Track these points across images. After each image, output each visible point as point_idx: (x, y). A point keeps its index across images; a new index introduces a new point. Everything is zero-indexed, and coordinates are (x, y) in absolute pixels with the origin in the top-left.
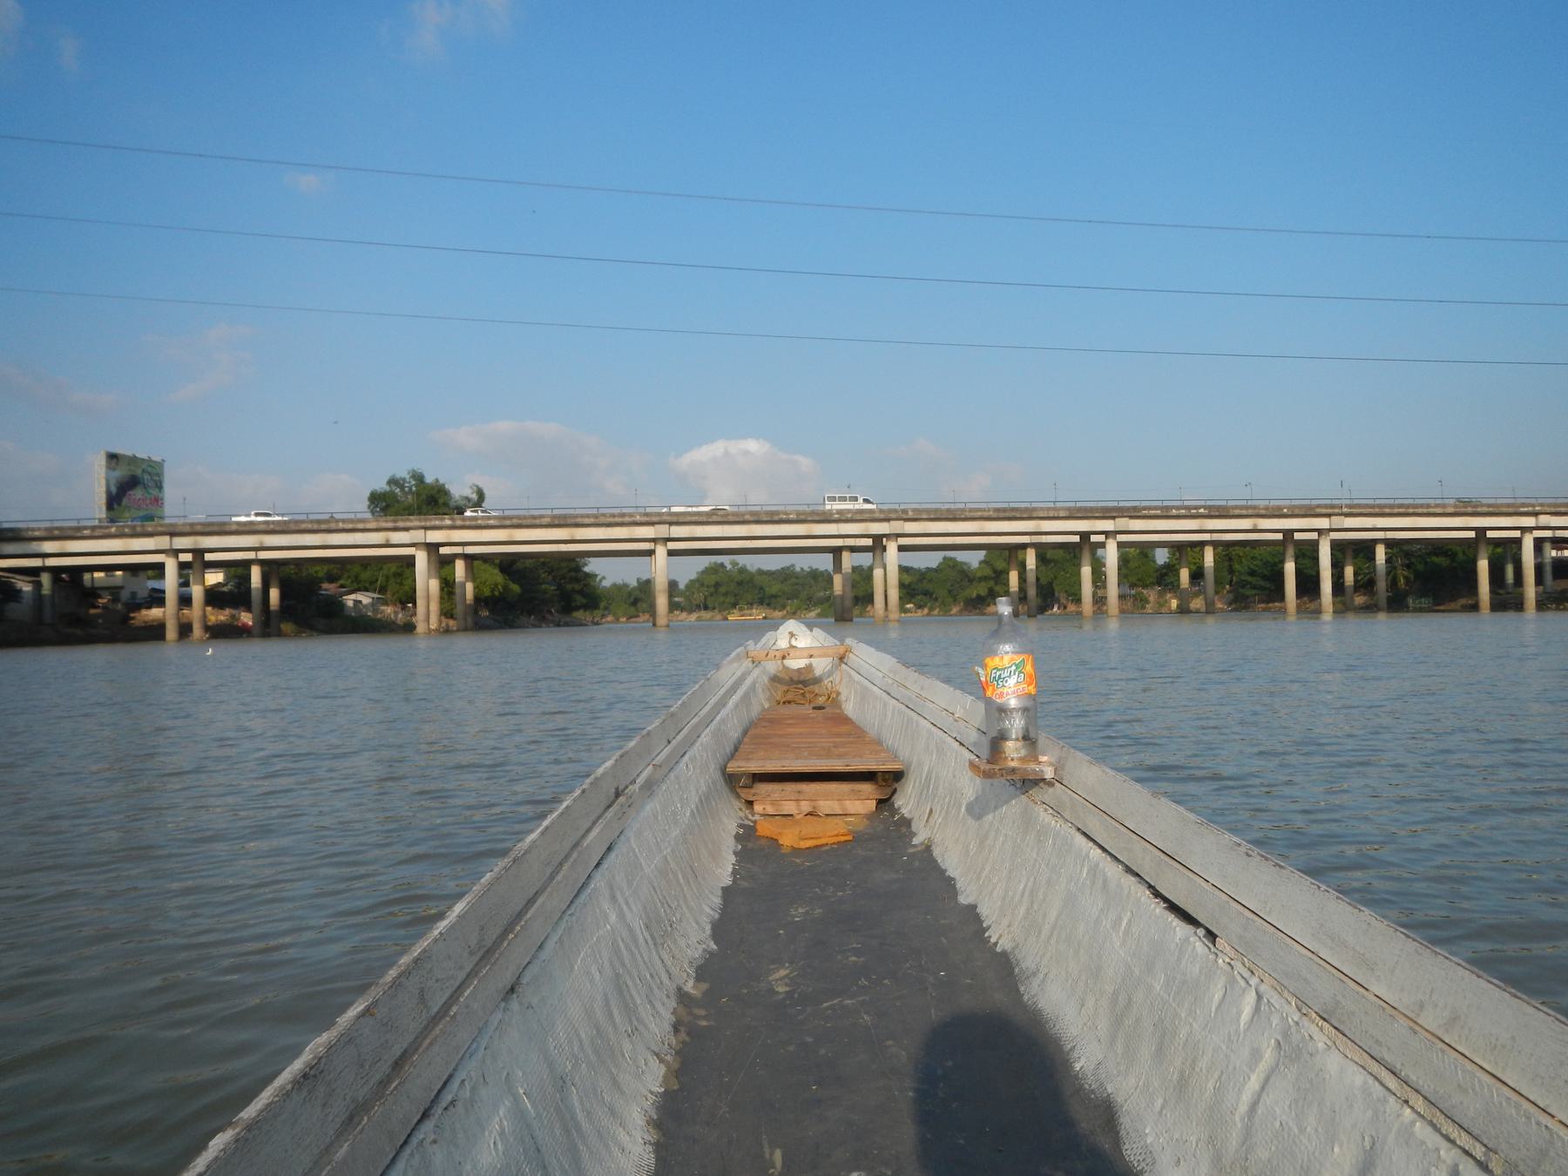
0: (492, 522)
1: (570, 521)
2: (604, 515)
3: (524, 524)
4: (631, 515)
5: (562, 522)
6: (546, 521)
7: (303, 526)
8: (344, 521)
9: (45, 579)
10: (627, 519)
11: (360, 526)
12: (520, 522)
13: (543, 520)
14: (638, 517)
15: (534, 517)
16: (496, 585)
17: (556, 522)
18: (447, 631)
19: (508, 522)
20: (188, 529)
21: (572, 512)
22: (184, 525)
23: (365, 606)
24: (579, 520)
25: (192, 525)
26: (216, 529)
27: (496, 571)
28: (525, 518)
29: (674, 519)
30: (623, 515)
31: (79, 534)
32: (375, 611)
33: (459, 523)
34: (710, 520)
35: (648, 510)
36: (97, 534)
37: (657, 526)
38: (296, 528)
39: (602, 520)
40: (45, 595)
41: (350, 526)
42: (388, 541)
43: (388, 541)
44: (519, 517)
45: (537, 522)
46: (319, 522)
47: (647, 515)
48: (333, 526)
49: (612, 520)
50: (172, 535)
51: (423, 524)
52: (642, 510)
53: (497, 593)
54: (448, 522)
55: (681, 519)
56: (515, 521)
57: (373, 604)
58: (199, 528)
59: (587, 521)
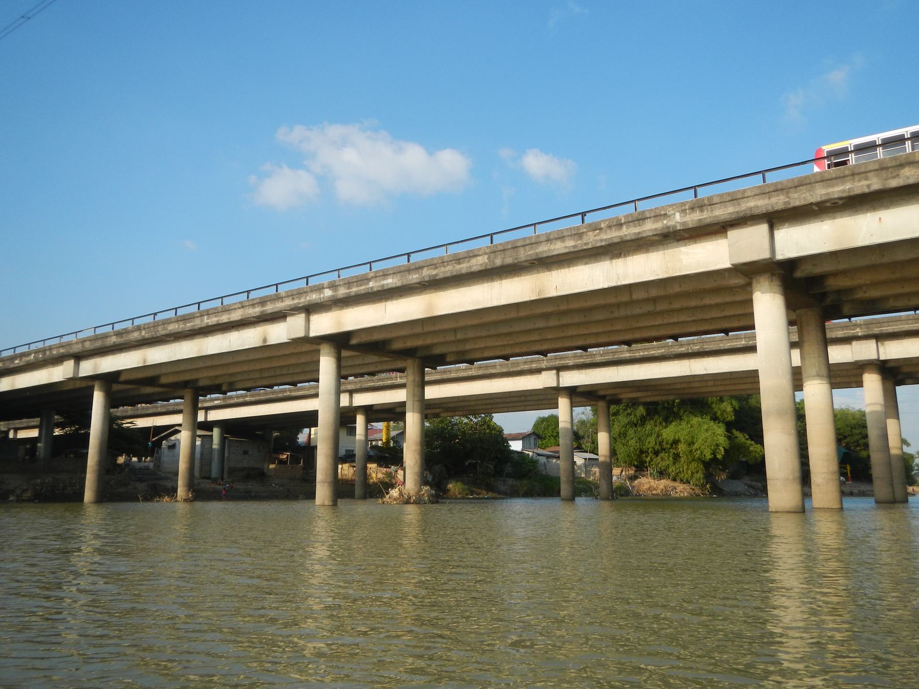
0: (390, 282)
1: (524, 255)
2: (595, 227)
3: (441, 276)
4: (658, 216)
5: (509, 260)
6: (478, 263)
7: (172, 327)
8: (208, 313)
9: (216, 432)
10: (650, 227)
11: (224, 318)
12: (434, 272)
13: (474, 261)
14: (678, 216)
15: (458, 259)
16: (717, 445)
17: (498, 262)
18: (419, 502)
19: (414, 278)
20: (77, 349)
21: (529, 232)
22: (76, 343)
23: (579, 467)
24: (544, 249)
25: (83, 341)
26: (98, 344)
27: (719, 430)
28: (443, 262)
29: (778, 202)
30: (641, 219)
31: (12, 366)
32: (587, 472)
33: (342, 292)
34: (894, 183)
35: (703, 193)
36: (21, 364)
37: (733, 234)
38: (164, 332)
39: (592, 239)
40: (215, 449)
41: (212, 320)
42: (265, 340)
43: (265, 340)
44: (432, 264)
45: (464, 267)
46: (185, 319)
47: (700, 206)
48: (197, 323)
49: (613, 235)
50: (78, 357)
51: (296, 301)
52: (689, 196)
53: (719, 456)
54: (328, 293)
55: (799, 198)
56: (427, 273)
57: (585, 465)
58: (88, 345)
59: (559, 248)
